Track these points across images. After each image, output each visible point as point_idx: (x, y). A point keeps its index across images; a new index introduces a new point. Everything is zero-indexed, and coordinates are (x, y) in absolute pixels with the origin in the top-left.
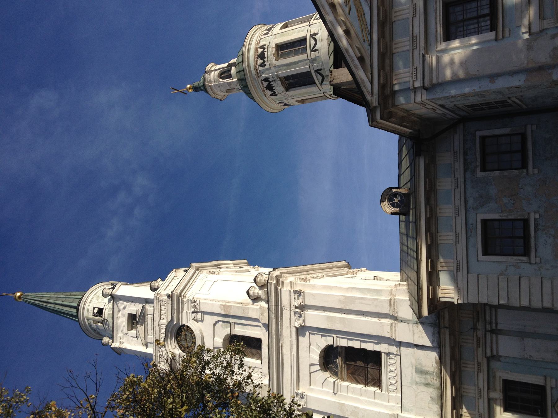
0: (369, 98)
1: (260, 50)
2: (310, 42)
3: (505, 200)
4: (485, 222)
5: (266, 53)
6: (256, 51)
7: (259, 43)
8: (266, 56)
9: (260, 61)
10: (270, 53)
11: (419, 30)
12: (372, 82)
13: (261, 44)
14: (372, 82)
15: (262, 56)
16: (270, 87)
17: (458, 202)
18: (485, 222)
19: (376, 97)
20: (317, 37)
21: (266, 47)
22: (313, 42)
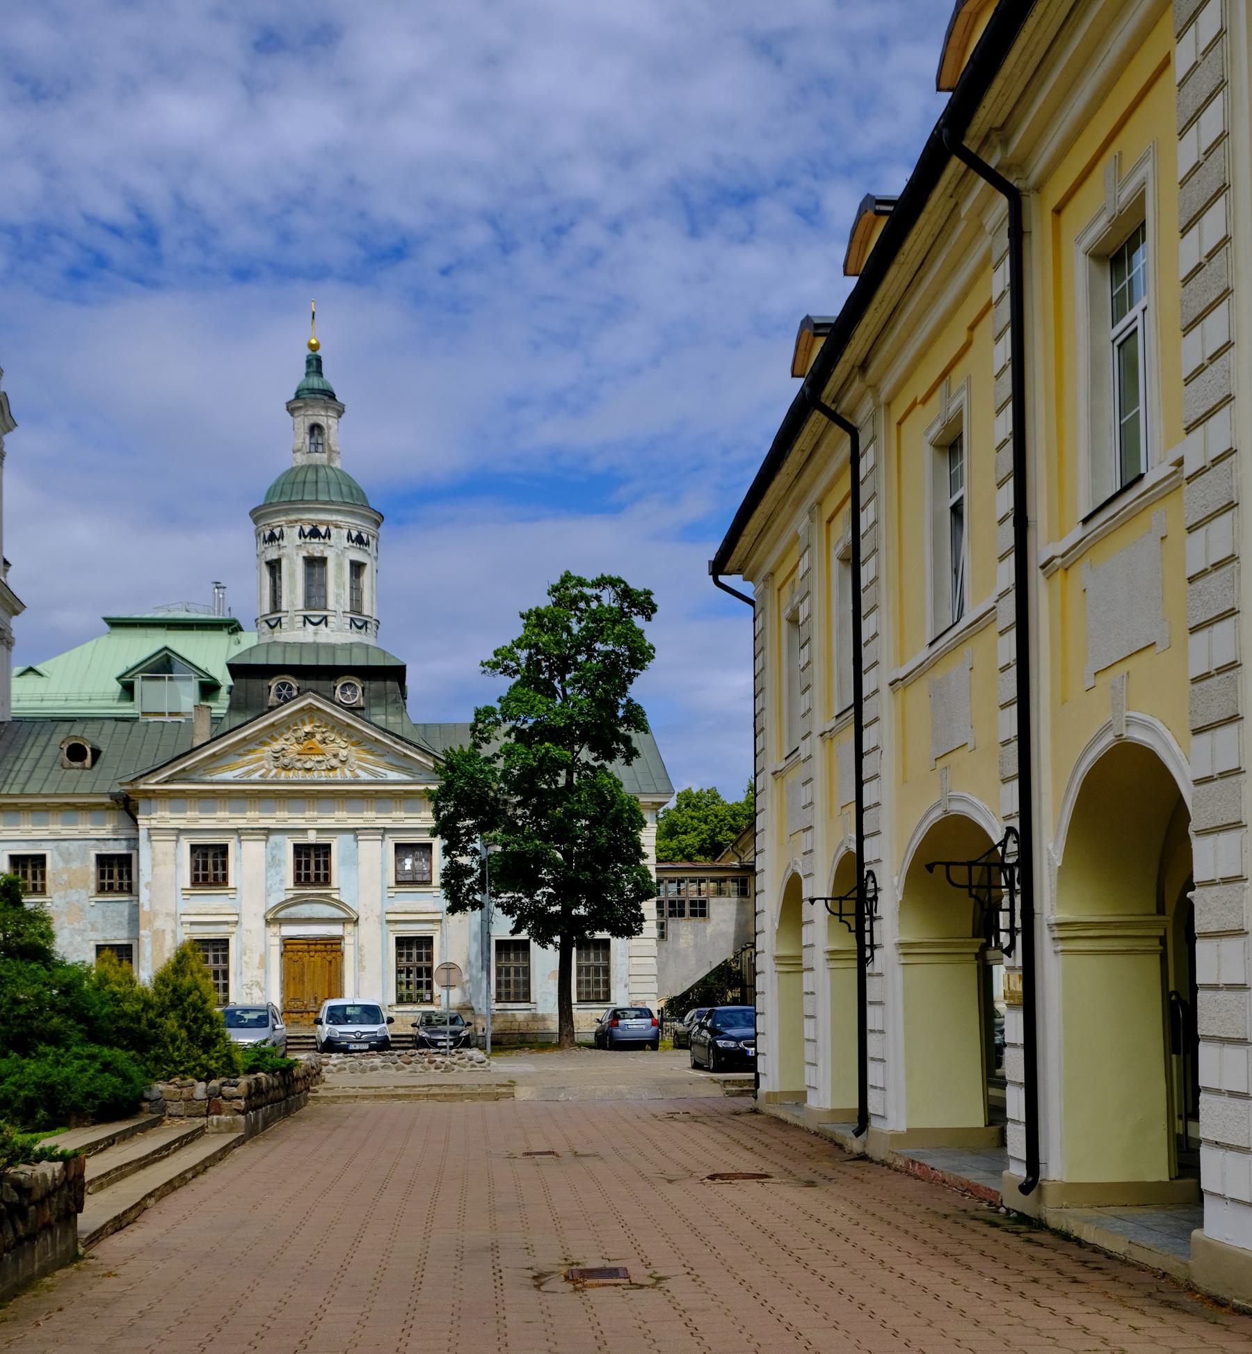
0: (142, 780)
1: (323, 530)
2: (316, 615)
3: (65, 877)
4: (43, 857)
5: (317, 540)
6: (322, 522)
7: (337, 527)
8: (313, 540)
9: (307, 529)
10: (316, 548)
11: (204, 824)
12: (157, 783)
13: (333, 531)
14: (157, 783)
15: (315, 533)
16: (272, 538)
17: (64, 832)
18: (43, 857)
19: (142, 787)
20: (322, 626)
21: (327, 540)
22: (315, 620)
